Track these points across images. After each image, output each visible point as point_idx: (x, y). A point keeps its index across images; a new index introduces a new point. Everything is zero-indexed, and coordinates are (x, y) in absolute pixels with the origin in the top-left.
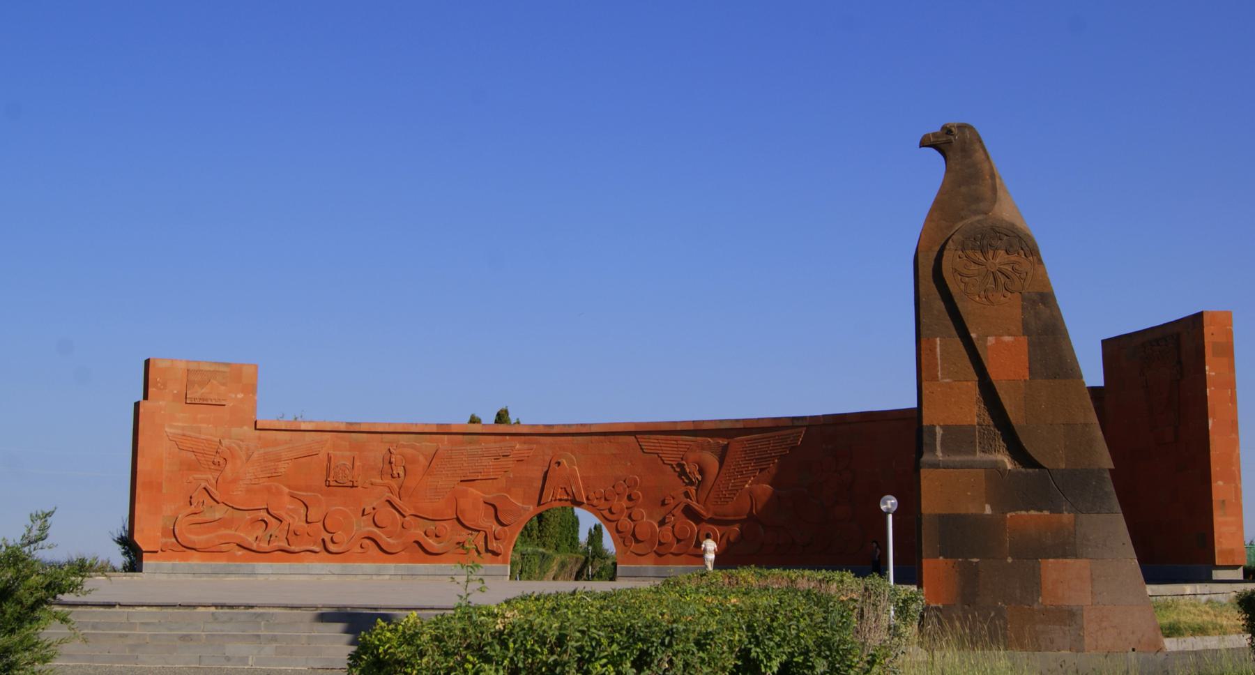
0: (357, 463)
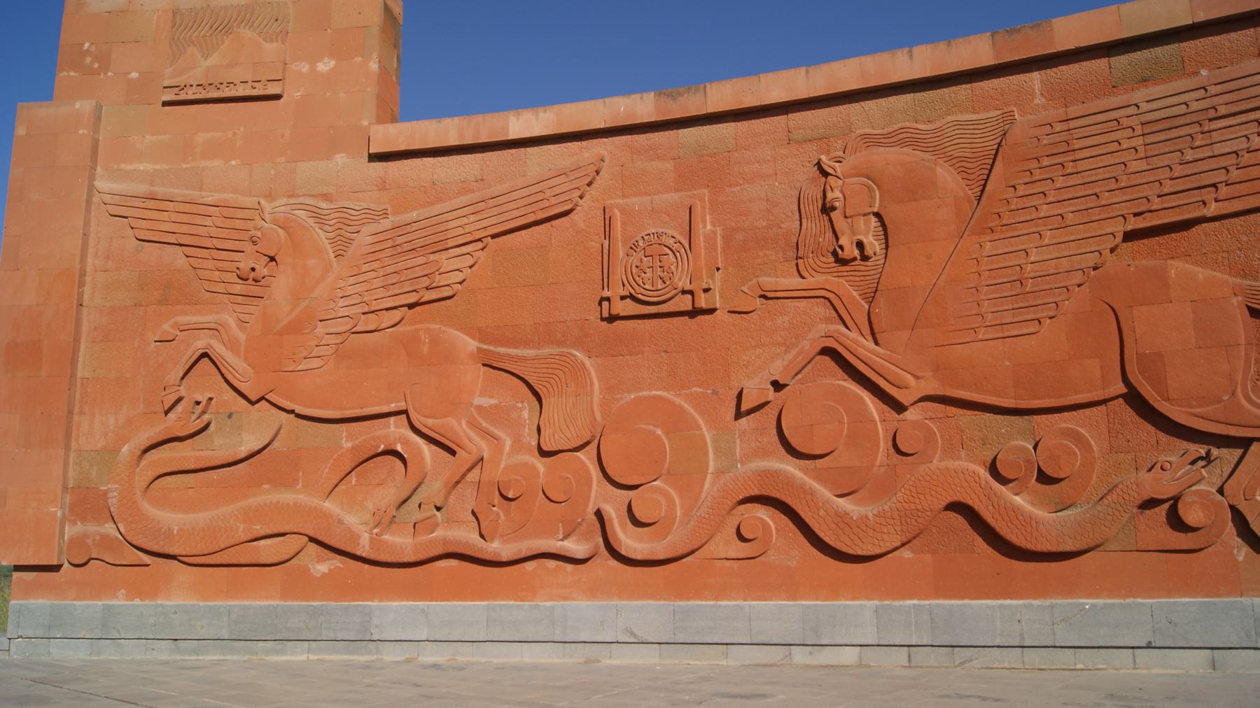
0: (706, 227)
